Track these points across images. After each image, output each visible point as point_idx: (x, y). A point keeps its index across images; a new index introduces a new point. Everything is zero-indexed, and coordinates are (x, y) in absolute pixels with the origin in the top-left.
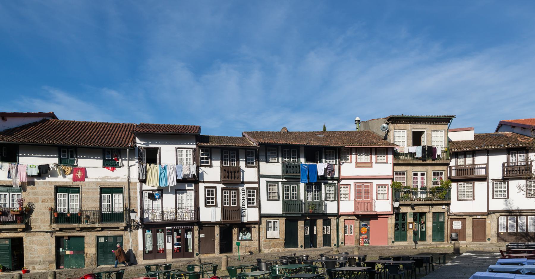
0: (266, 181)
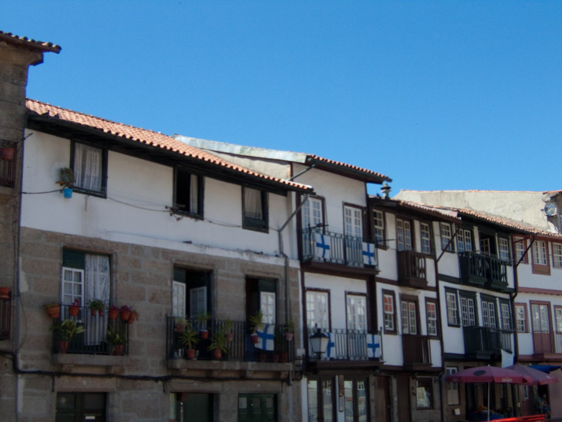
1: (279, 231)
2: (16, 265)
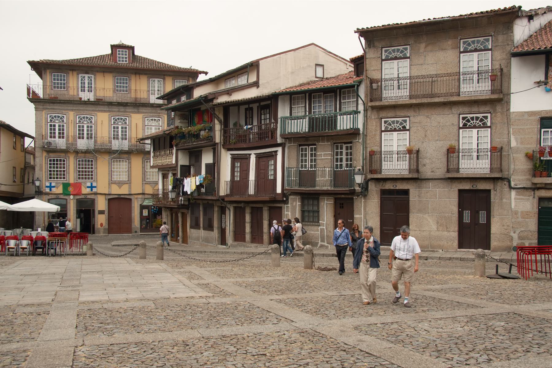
2: (509, 132)
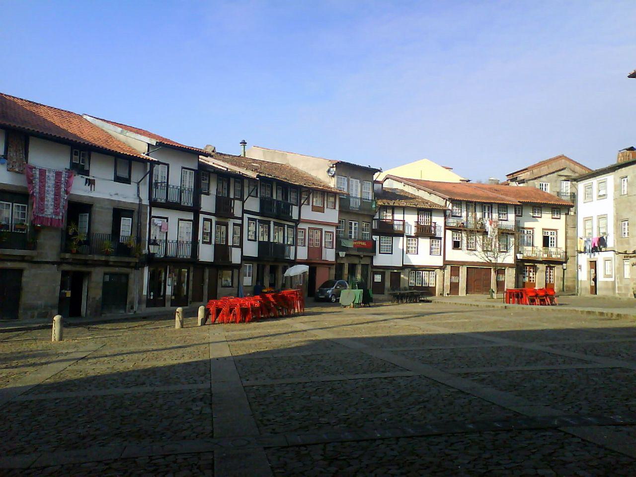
0: (248, 217)
1: (138, 183)
